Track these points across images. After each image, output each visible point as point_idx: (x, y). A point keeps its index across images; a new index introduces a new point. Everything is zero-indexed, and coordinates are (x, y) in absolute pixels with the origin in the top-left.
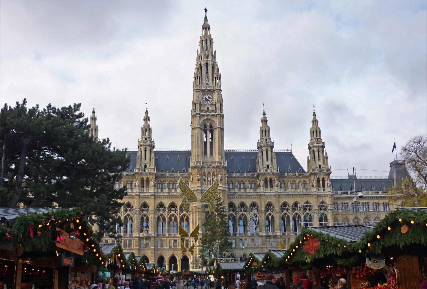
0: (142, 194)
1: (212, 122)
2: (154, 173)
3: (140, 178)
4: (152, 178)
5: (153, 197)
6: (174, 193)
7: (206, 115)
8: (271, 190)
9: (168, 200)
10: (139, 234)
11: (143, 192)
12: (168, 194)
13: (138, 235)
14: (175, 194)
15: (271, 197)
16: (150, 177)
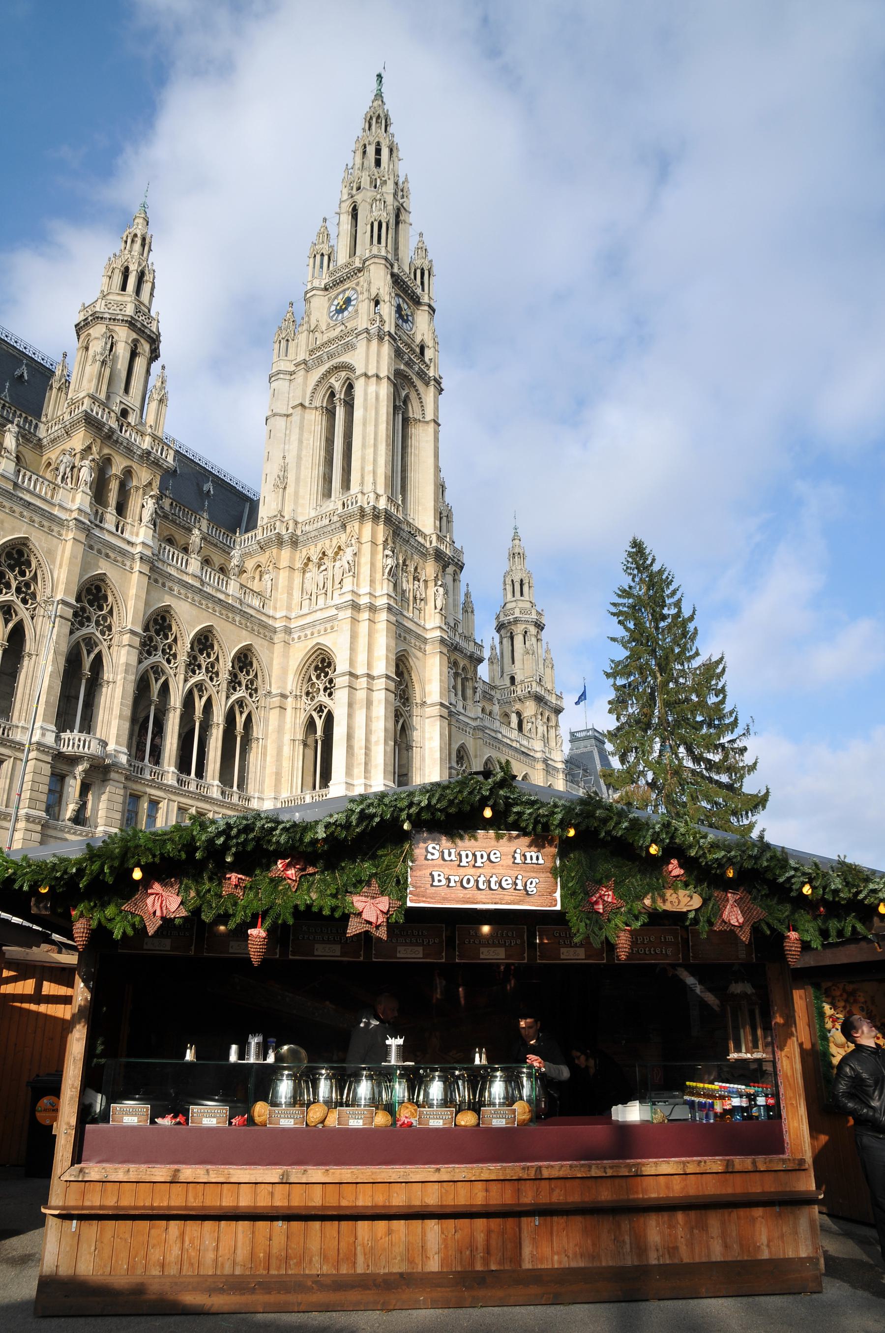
0: (97, 532)
1: (413, 396)
2: (165, 465)
3: (99, 454)
4: (150, 483)
5: (146, 569)
6: (218, 590)
7: (406, 357)
8: (465, 708)
9: (194, 611)
10: (58, 738)
11: (98, 522)
12: (198, 585)
13: (50, 739)
14: (222, 597)
15: (466, 732)
16: (143, 475)
